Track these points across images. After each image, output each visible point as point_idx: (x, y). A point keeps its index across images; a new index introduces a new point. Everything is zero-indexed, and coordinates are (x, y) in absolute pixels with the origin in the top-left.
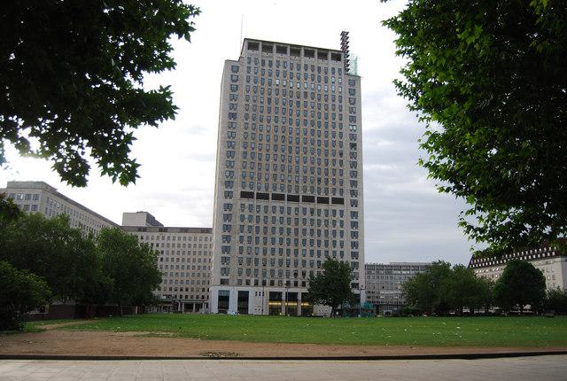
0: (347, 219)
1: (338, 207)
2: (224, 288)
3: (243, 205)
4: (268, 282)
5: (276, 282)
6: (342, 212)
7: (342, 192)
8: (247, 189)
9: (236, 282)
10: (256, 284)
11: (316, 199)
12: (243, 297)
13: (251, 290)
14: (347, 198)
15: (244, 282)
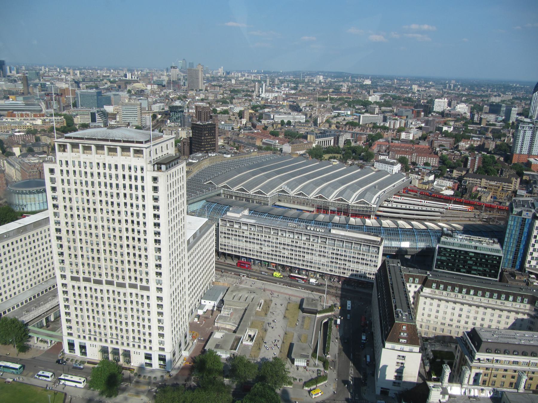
0: (154, 302)
1: (145, 293)
2: (71, 338)
3: (73, 287)
4: (98, 339)
5: (103, 340)
6: (148, 297)
7: (147, 281)
8: (75, 275)
9: (77, 336)
10: (90, 338)
11: (127, 285)
12: (83, 347)
13: (88, 343)
14: (153, 286)
15: (82, 337)
